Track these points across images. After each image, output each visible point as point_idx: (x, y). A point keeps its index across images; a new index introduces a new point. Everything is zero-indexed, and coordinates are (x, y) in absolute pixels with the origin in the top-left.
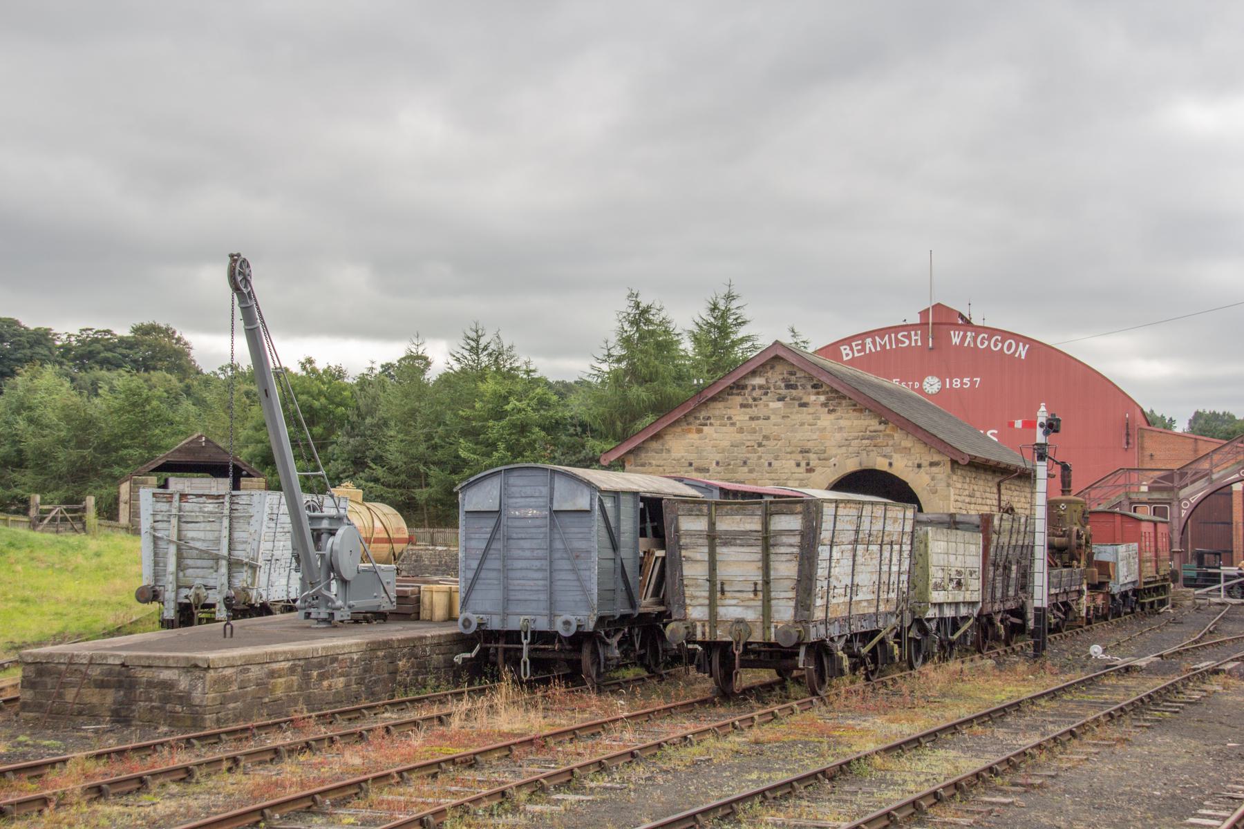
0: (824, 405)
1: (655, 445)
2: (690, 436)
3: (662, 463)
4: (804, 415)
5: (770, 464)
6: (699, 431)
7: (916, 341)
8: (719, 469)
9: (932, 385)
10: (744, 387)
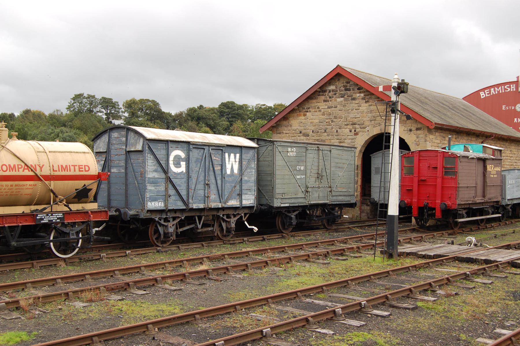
0: (363, 99)
1: (285, 123)
2: (301, 118)
3: (288, 132)
4: (353, 105)
5: (337, 131)
6: (305, 115)
8: (314, 134)
10: (325, 91)
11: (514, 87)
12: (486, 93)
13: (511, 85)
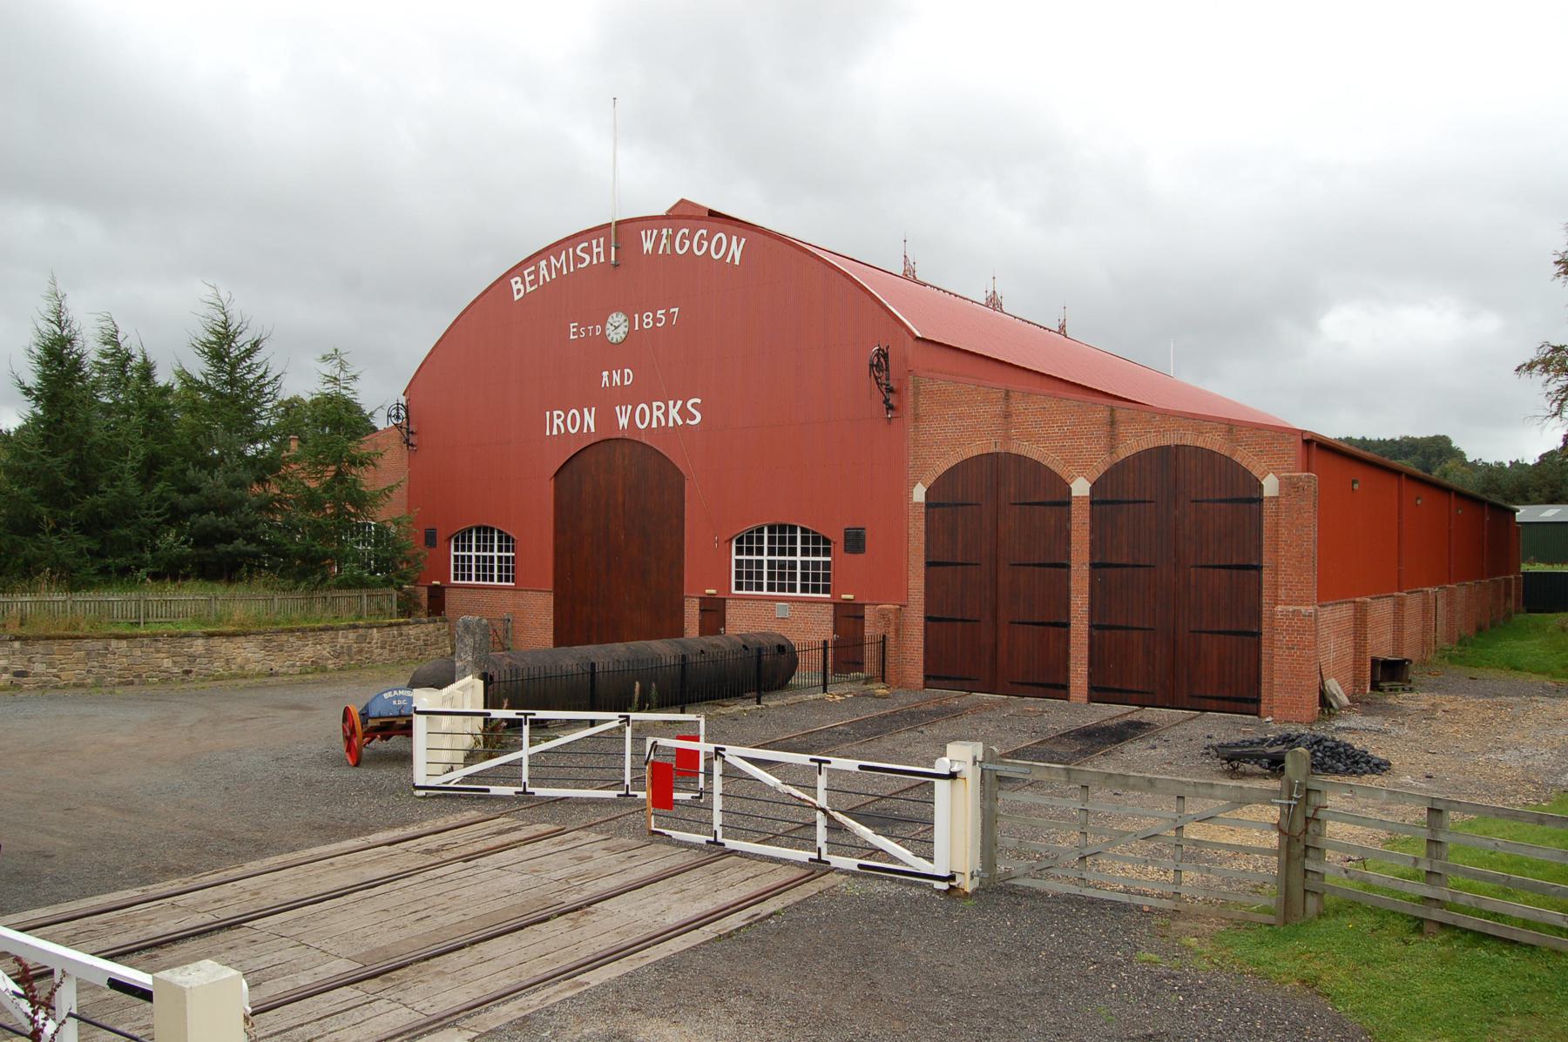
9: (617, 328)
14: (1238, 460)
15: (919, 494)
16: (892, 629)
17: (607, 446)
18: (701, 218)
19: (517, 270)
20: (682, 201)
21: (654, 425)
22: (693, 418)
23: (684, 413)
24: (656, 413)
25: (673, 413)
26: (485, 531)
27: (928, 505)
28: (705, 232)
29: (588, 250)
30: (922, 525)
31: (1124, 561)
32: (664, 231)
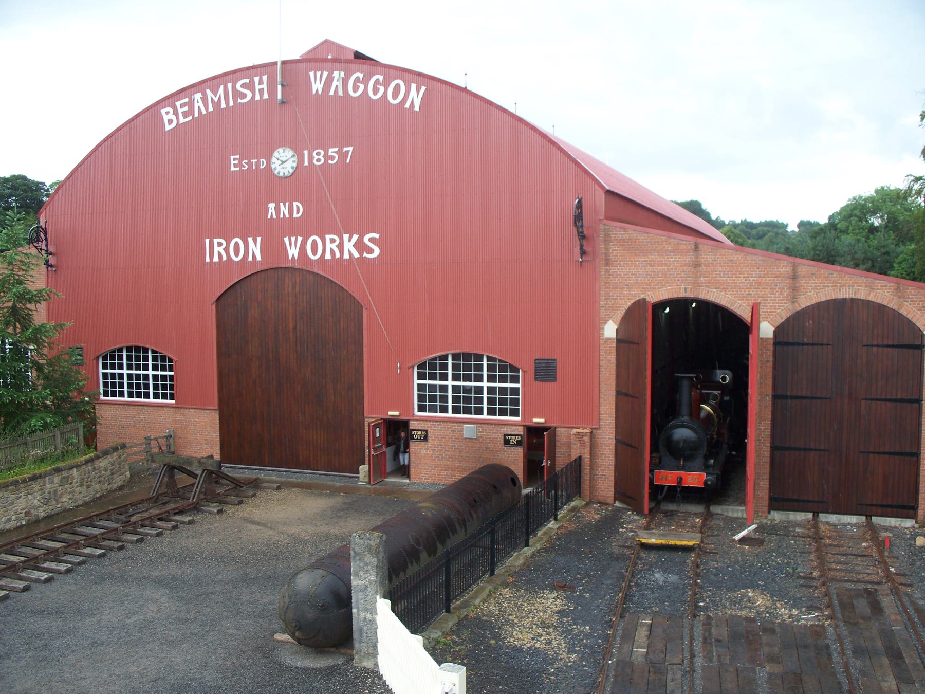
7: (261, 91)
9: (283, 162)
11: (264, 86)
12: (180, 111)
13: (257, 79)
14: (905, 313)
15: (610, 330)
16: (587, 450)
17: (274, 275)
18: (348, 61)
19: (169, 100)
20: (327, 42)
21: (328, 256)
22: (371, 251)
23: (360, 246)
24: (329, 246)
25: (349, 246)
26: (137, 353)
27: (619, 341)
28: (381, 78)
29: (250, 86)
30: (612, 358)
31: (804, 394)
32: (336, 74)
